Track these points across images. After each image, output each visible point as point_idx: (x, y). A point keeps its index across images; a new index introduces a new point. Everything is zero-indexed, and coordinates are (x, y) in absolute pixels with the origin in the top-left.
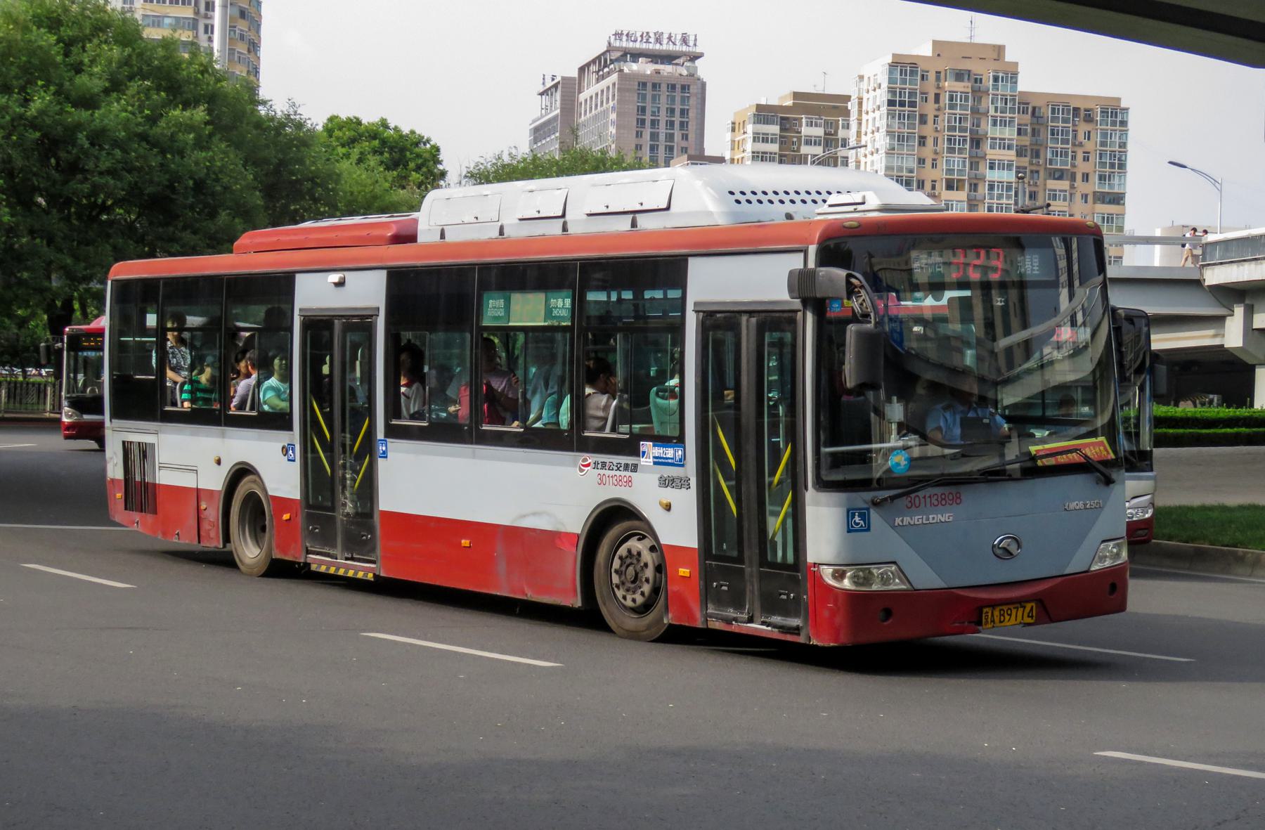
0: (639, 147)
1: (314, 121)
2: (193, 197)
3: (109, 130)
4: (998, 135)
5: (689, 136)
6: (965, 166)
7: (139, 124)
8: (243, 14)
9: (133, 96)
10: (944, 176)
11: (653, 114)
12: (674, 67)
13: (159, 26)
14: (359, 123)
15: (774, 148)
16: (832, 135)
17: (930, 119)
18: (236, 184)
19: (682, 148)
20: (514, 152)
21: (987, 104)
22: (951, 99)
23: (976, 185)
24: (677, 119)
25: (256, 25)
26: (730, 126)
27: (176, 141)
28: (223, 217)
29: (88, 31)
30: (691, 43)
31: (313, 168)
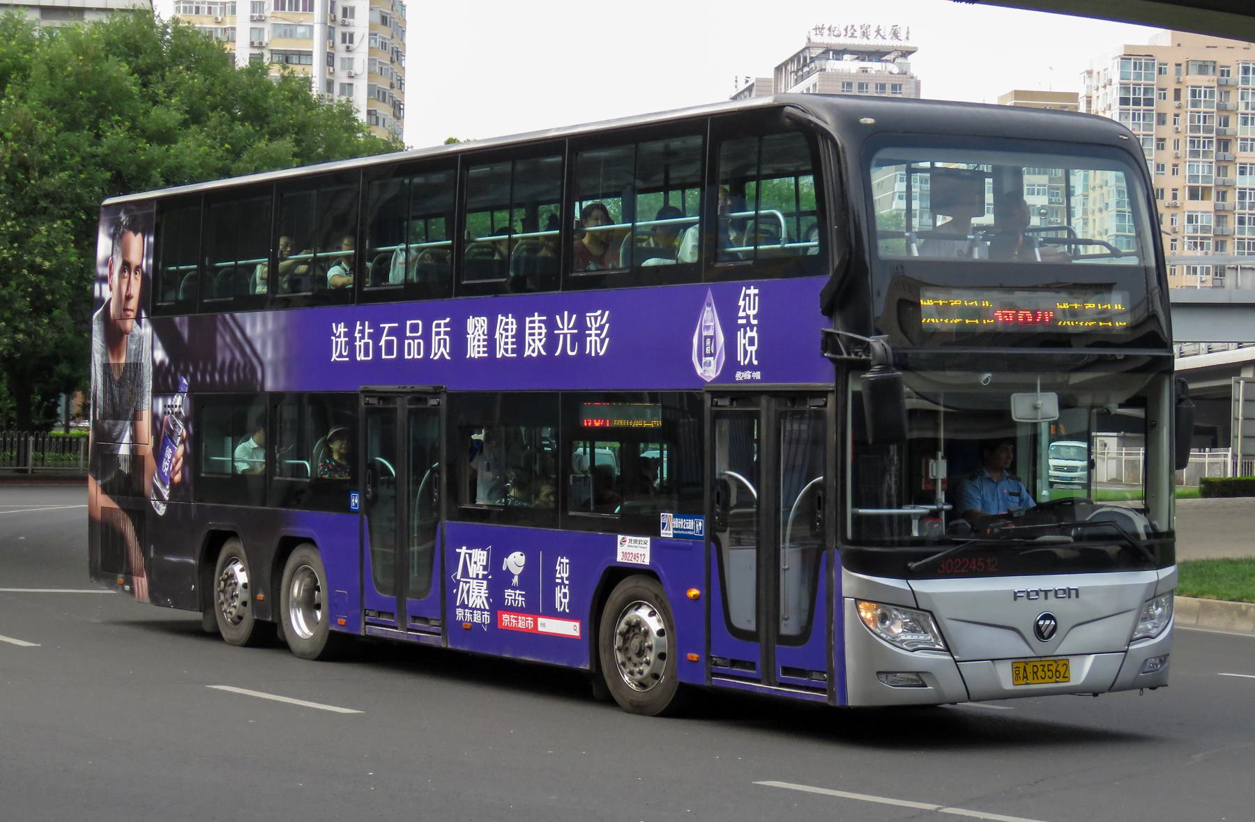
3: (182, 167)
4: (1249, 136)
6: (1210, 171)
8: (384, 20)
9: (215, 128)
10: (1187, 184)
12: (884, 64)
13: (291, 36)
17: (1170, 119)
21: (1235, 99)
22: (1194, 94)
23: (1224, 193)
25: (400, 31)
29: (167, 59)
30: (902, 35)
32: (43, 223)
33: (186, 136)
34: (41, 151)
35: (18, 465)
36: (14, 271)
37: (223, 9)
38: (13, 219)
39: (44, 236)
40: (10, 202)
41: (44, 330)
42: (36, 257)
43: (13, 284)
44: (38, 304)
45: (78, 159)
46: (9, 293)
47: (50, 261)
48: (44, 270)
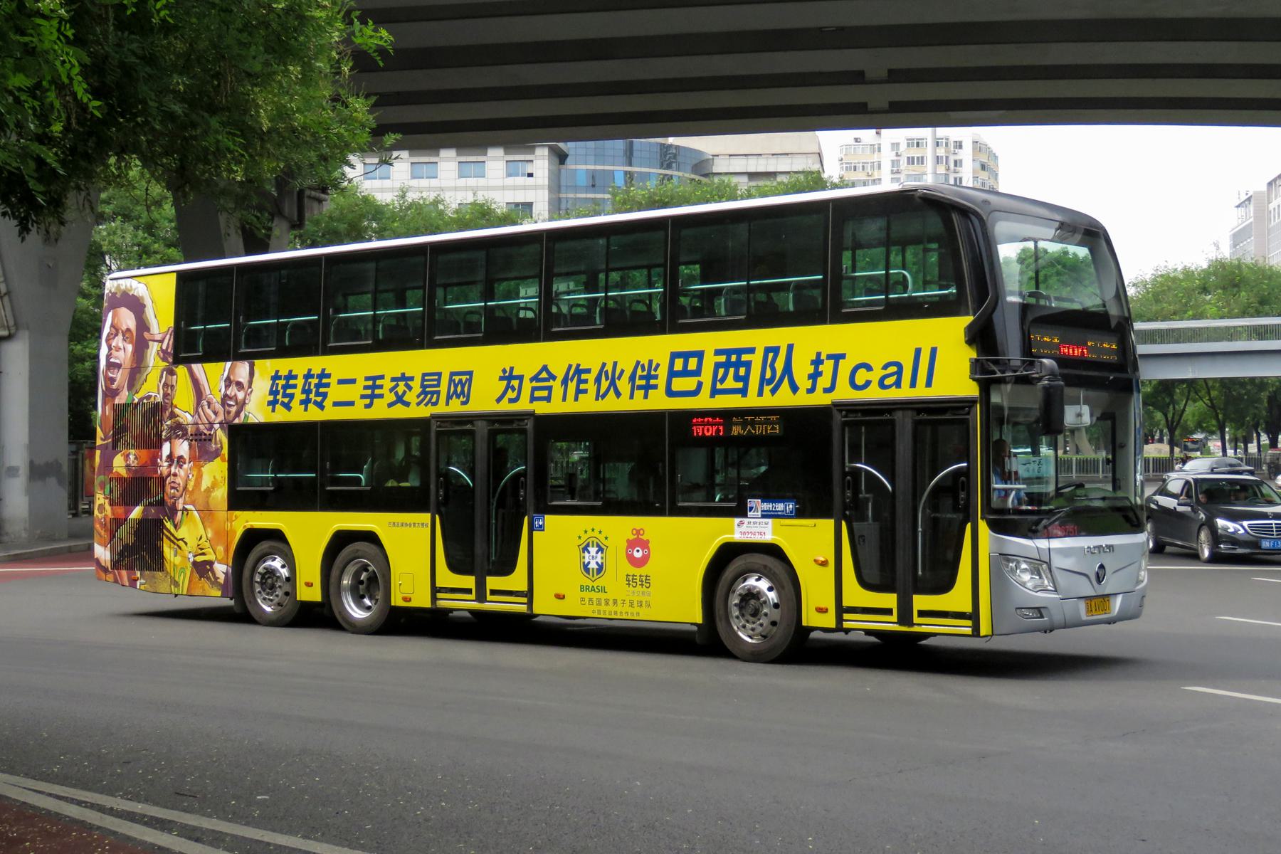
8: (983, 167)
20: (1166, 264)
37: (872, 167)
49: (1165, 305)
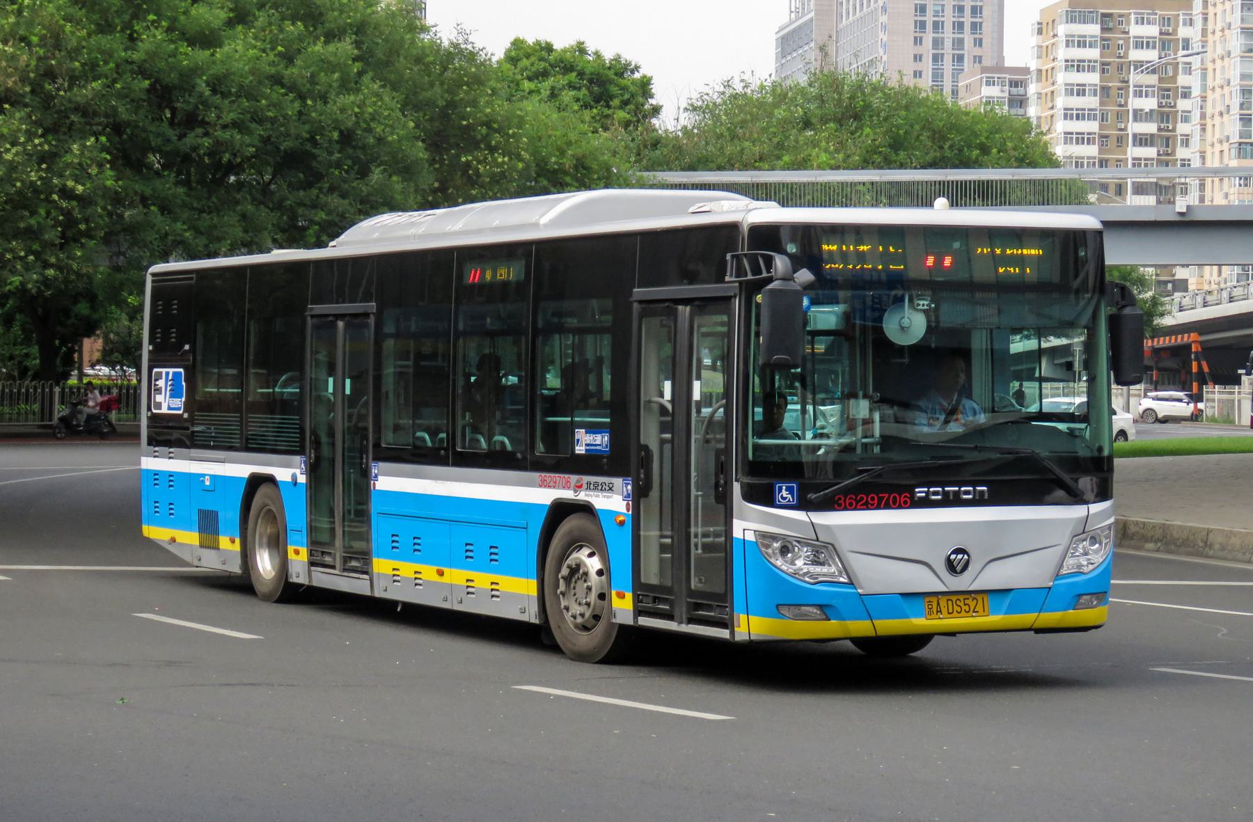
0: (918, 58)
1: (489, 50)
2: (338, 153)
3: (234, 74)
5: (984, 41)
7: (272, 64)
11: (936, 14)
14: (549, 48)
15: (1094, 54)
16: (1169, 34)
18: (392, 134)
19: (975, 57)
24: (967, 19)
26: (1036, 26)
27: (317, 84)
28: (376, 175)
31: (488, 110)
32: (75, 142)
33: (234, 38)
34: (72, 59)
35: (42, 421)
36: (42, 197)
38: (42, 136)
39: (75, 156)
40: (36, 116)
41: (78, 263)
42: (67, 180)
43: (42, 212)
44: (69, 234)
45: (112, 65)
46: (39, 223)
47: (83, 185)
48: (77, 195)
49: (747, 144)
